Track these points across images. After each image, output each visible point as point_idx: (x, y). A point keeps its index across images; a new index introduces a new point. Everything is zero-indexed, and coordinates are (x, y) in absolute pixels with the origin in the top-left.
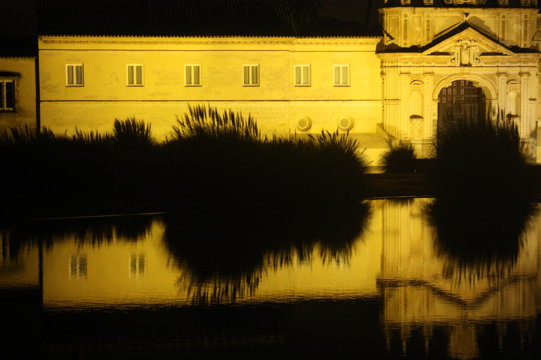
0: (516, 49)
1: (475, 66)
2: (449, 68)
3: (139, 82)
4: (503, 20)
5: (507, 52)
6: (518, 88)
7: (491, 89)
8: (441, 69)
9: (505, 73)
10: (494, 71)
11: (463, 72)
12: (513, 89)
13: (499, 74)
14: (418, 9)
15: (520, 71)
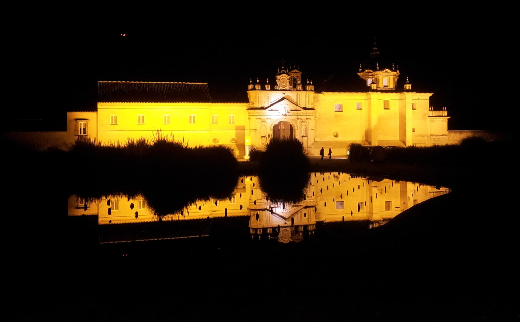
0: (305, 108)
3: (143, 122)
10: (296, 117)
13: (298, 119)
14: (263, 91)
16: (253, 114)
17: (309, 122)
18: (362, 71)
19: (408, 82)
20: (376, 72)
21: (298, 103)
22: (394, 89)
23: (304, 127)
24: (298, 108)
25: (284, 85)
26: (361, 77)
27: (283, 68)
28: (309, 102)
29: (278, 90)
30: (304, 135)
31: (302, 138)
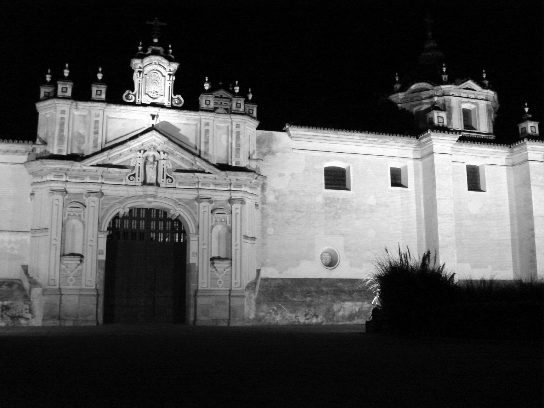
0: (224, 167)
1: (164, 186)
2: (125, 188)
4: (207, 128)
5: (210, 169)
6: (228, 220)
7: (189, 219)
8: (113, 188)
9: (209, 199)
10: (194, 194)
11: (145, 193)
12: (222, 221)
14: (81, 104)
15: (231, 198)
16: (42, 177)
17: (238, 211)
18: (402, 90)
19: (530, 116)
20: (442, 87)
21: (203, 149)
22: (492, 137)
23: (219, 228)
24: (200, 164)
25: (157, 90)
26: (400, 105)
27: (156, 41)
28: (238, 149)
29: (134, 104)
30: (222, 256)
31: (213, 264)
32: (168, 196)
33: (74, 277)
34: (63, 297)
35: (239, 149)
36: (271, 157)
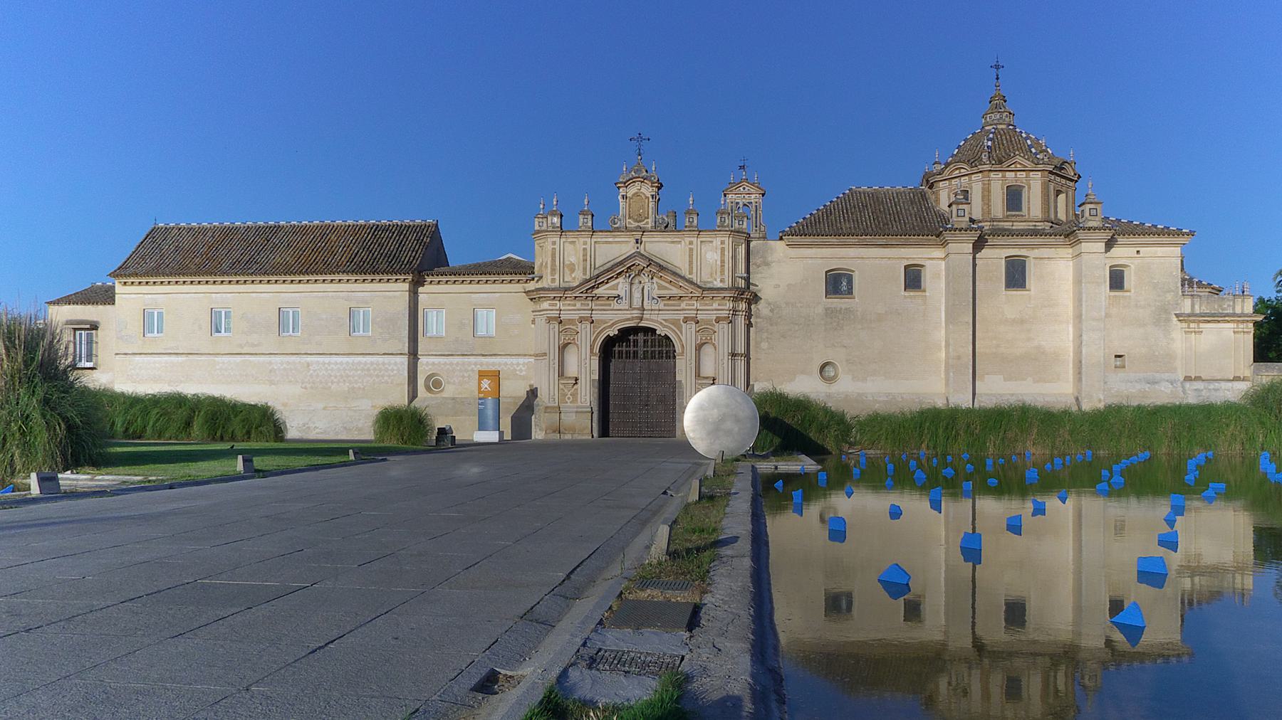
4: (690, 246)
13: (686, 320)
32: (654, 317)
33: (571, 395)
34: (562, 414)
35: (724, 266)
36: (765, 268)
